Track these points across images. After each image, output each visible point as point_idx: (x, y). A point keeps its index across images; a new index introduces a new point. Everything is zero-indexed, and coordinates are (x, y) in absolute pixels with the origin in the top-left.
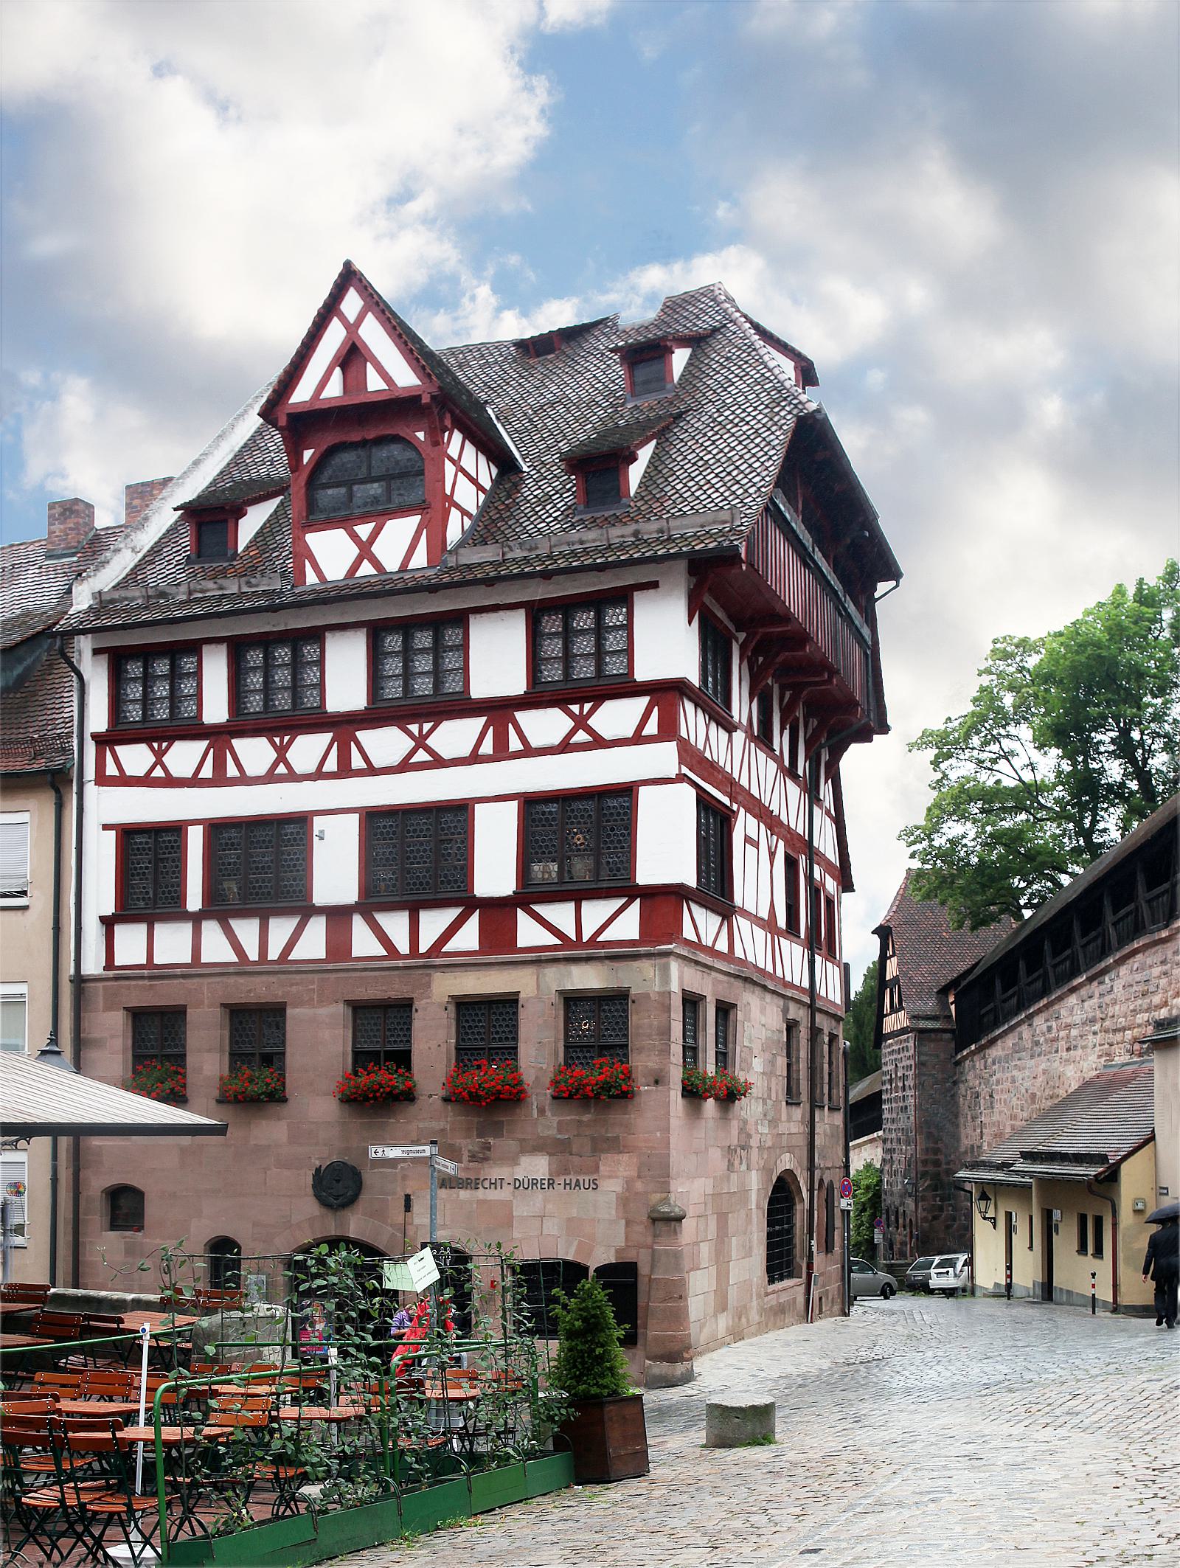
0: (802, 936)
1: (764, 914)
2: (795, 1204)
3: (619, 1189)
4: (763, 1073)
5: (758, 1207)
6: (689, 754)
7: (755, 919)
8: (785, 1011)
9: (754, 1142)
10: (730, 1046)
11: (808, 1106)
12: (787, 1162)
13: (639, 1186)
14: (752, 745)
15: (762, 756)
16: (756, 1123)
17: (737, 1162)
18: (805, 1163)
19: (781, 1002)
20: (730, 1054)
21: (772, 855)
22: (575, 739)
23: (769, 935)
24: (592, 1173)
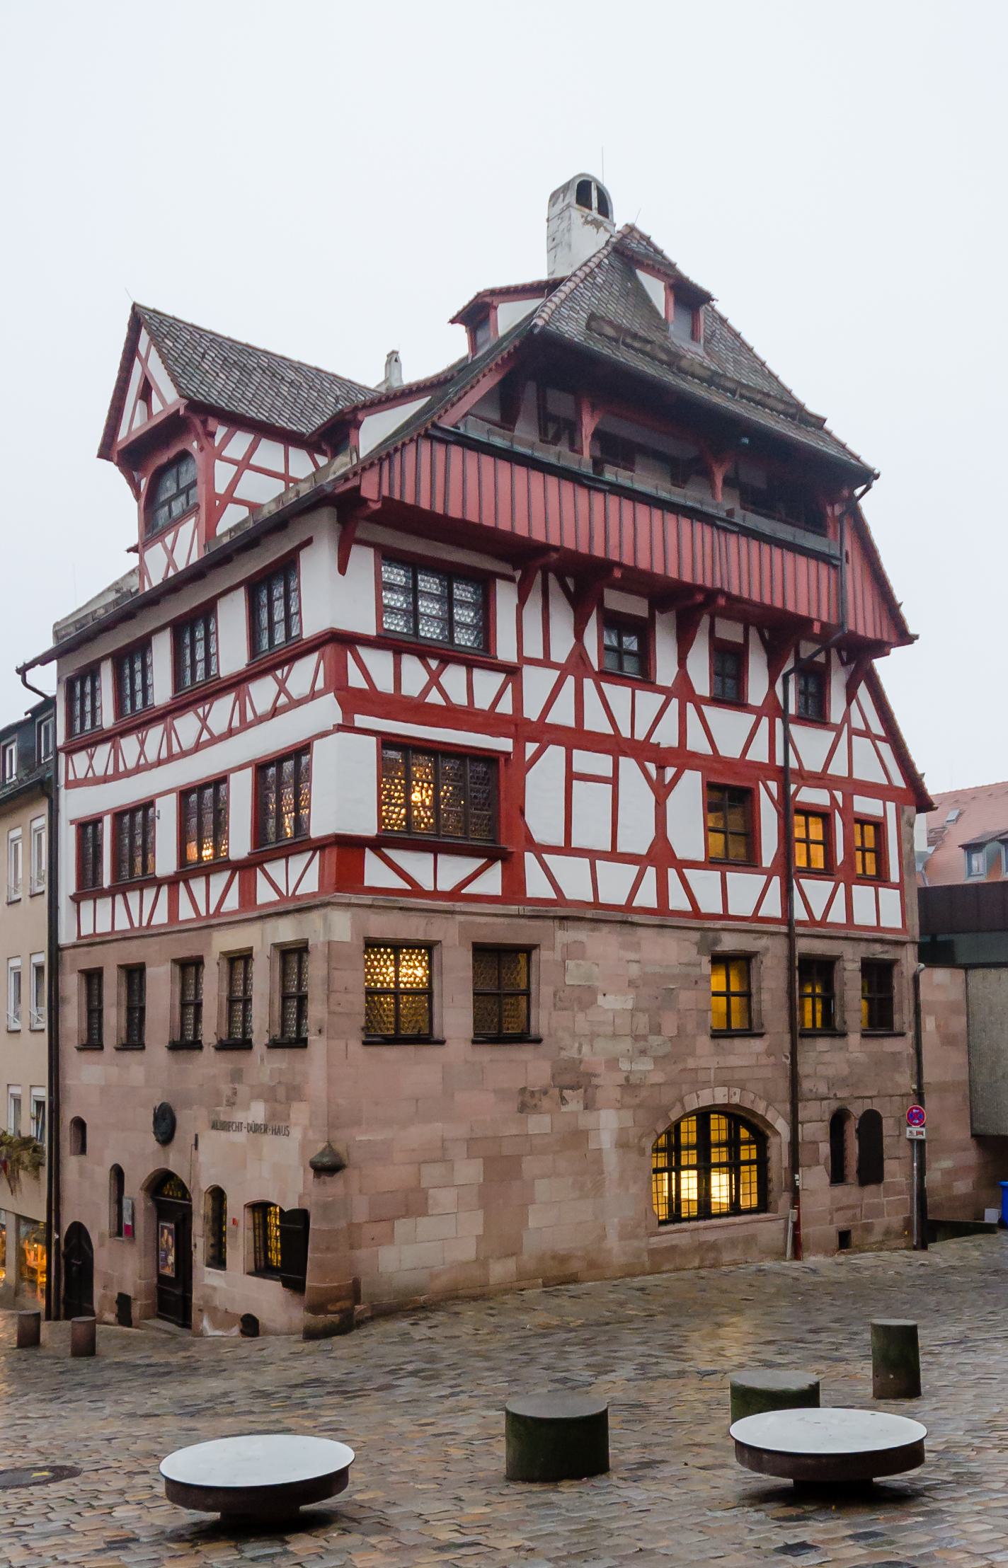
1: (643, 850)
3: (300, 1137)
4: (634, 1011)
6: (368, 701)
7: (614, 855)
9: (608, 1084)
10: (533, 987)
11: (787, 1038)
13: (311, 1135)
14: (589, 684)
16: (613, 1064)
19: (696, 936)
20: (533, 995)
21: (661, 791)
22: (279, 703)
23: (651, 872)
24: (285, 1120)
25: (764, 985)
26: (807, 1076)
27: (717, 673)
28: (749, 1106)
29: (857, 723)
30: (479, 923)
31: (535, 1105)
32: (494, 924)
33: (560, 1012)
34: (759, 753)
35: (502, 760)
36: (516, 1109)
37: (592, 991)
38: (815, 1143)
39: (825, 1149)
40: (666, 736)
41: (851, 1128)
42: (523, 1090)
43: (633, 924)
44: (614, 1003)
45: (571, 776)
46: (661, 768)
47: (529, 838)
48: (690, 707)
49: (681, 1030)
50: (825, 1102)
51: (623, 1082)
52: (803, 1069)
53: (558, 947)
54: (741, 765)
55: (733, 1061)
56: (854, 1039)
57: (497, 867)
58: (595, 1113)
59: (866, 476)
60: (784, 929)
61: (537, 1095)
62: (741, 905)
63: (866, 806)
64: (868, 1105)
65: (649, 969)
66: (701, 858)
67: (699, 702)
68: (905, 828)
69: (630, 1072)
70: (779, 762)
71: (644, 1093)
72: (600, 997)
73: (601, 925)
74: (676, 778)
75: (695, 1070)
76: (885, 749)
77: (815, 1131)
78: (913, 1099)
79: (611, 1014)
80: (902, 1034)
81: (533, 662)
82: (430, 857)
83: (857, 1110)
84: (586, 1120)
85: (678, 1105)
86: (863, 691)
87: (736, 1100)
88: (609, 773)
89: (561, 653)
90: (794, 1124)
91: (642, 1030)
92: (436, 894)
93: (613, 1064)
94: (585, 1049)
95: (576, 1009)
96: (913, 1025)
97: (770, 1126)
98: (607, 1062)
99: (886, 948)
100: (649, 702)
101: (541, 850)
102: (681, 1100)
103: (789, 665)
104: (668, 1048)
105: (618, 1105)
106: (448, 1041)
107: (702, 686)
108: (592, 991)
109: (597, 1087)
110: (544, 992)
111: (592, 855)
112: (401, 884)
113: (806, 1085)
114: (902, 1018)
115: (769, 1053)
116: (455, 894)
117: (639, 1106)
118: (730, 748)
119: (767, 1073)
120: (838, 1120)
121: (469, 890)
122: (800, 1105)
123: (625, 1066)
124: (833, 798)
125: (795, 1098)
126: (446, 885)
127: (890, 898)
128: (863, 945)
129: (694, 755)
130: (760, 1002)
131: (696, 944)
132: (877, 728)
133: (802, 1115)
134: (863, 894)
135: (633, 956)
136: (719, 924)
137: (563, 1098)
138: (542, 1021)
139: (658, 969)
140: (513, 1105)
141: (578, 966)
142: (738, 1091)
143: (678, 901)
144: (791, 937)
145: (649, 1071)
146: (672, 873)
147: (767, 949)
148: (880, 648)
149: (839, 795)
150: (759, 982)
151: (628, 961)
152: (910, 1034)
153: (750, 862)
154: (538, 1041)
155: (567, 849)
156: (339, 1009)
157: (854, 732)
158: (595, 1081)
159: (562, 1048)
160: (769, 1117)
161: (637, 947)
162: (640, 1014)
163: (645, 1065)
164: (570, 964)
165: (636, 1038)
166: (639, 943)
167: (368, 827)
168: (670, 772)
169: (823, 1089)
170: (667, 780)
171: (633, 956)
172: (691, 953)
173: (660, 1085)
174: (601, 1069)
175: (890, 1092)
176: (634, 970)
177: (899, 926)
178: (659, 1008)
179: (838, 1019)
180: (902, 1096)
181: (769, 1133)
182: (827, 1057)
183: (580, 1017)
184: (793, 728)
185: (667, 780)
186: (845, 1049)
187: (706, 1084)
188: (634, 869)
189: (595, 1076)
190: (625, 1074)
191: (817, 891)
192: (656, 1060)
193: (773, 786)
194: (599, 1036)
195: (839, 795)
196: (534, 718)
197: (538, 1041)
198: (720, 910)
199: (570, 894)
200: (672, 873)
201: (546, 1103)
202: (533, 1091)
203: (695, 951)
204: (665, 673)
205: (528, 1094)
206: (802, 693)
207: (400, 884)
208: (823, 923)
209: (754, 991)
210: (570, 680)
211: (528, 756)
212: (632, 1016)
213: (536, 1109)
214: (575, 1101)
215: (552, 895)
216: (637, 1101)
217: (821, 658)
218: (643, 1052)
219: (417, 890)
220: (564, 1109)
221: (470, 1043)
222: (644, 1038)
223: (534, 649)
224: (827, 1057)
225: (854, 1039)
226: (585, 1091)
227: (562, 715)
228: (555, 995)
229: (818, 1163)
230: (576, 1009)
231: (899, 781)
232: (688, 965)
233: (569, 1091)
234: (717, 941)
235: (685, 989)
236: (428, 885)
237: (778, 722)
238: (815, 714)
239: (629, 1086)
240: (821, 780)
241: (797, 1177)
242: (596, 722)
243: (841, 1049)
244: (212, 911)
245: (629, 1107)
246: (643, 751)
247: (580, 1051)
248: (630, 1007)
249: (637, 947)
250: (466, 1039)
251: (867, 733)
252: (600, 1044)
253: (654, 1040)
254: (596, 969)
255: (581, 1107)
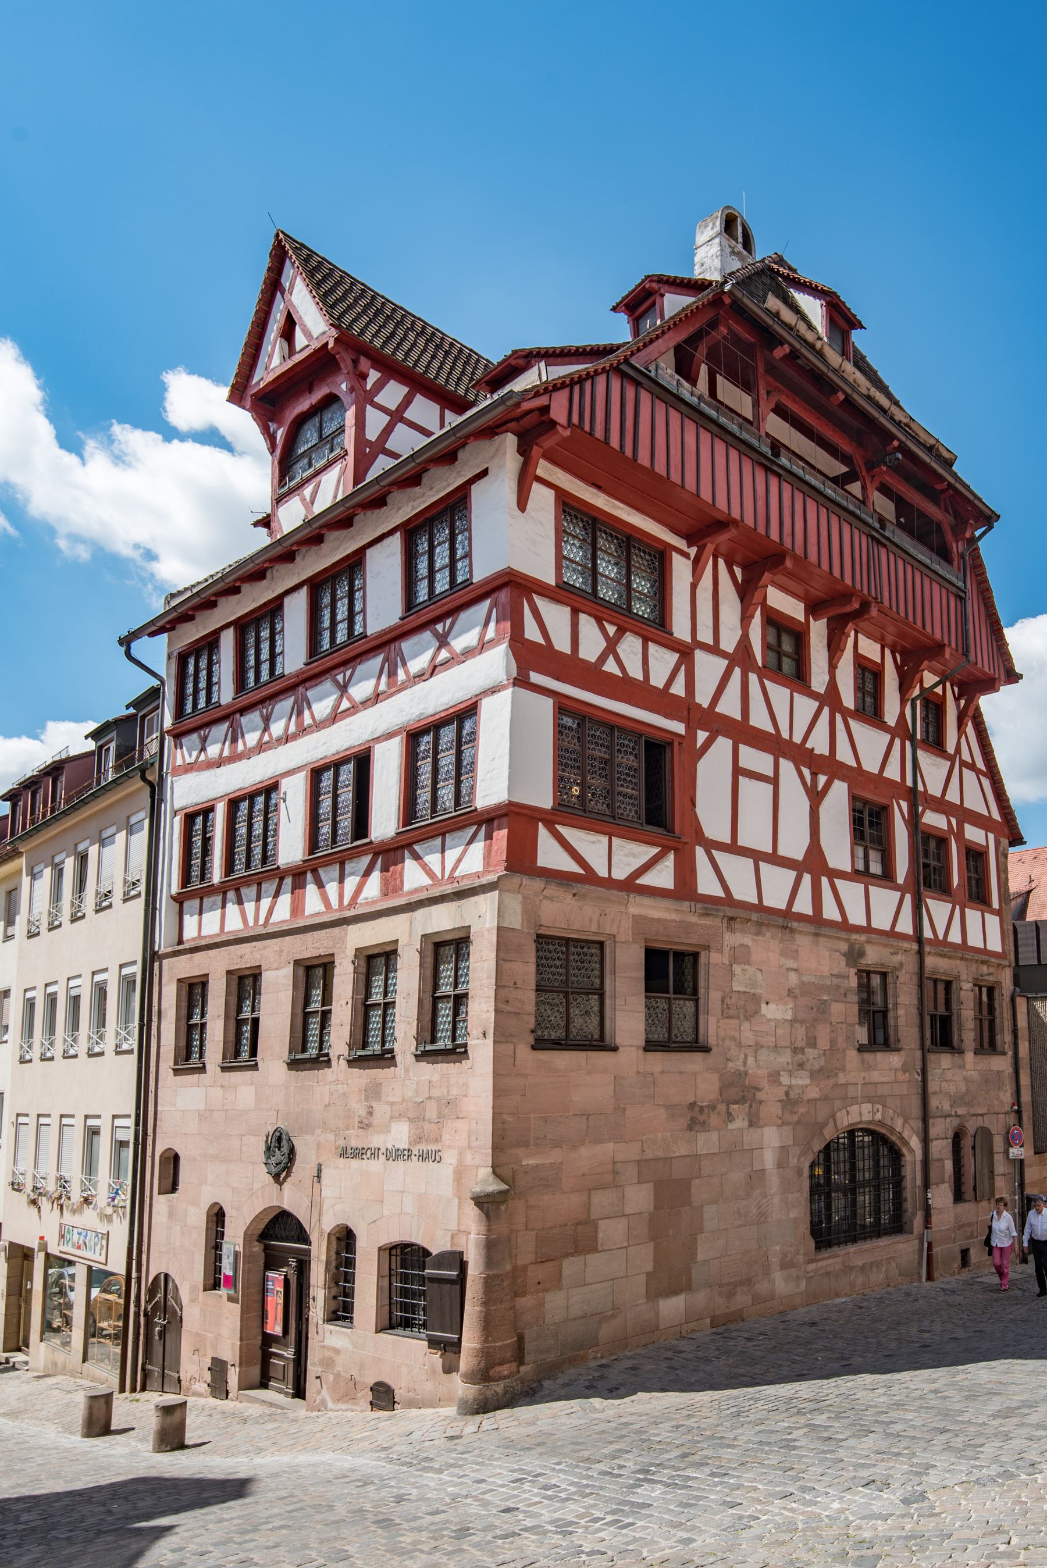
0: (900, 879)
2: (903, 1155)
4: (794, 1021)
5: (781, 1164)
7: (775, 859)
8: (854, 955)
9: (770, 1096)
11: (918, 1054)
12: (862, 1114)
15: (779, 694)
16: (774, 1077)
17: (714, 1120)
18: (916, 1110)
20: (702, 1001)
23: (807, 878)
25: (899, 1000)
26: (935, 1093)
27: (859, 689)
28: (889, 1123)
29: (966, 756)
30: (652, 919)
31: (704, 1122)
32: (666, 920)
33: (727, 1021)
34: (893, 772)
35: (676, 744)
36: (686, 1127)
37: (755, 999)
38: (941, 1160)
39: (949, 1165)
40: (819, 743)
41: (967, 1143)
42: (692, 1105)
43: (792, 931)
44: (775, 1012)
45: (738, 771)
46: (814, 775)
47: (699, 831)
48: (839, 718)
49: (833, 1042)
50: (948, 1120)
51: (784, 1098)
52: (932, 1086)
53: (726, 950)
54: (878, 780)
55: (876, 1076)
56: (969, 1056)
57: (671, 856)
58: (759, 1130)
59: (989, 519)
60: (915, 946)
61: (706, 1110)
62: (882, 921)
63: (974, 834)
64: (980, 1122)
65: (805, 979)
66: (849, 869)
67: (846, 713)
68: (1002, 857)
69: (790, 1087)
70: (909, 783)
71: (802, 1110)
72: (763, 1006)
73: (764, 929)
74: (828, 785)
75: (846, 1085)
76: (986, 783)
77: (941, 1148)
78: (1012, 1119)
79: (773, 1024)
80: (1004, 1054)
81: (704, 647)
82: (605, 839)
83: (971, 1127)
84: (750, 1137)
85: (831, 1120)
86: (970, 729)
87: (879, 1116)
88: (770, 773)
89: (729, 644)
90: (926, 1141)
91: (800, 1043)
92: (609, 883)
93: (774, 1077)
94: (751, 1060)
95: (742, 1018)
96: (1012, 1046)
97: (906, 1143)
98: (770, 1075)
99: (992, 970)
100: (806, 707)
101: (711, 846)
102: (833, 1117)
103: (917, 692)
104: (822, 1062)
105: (780, 1122)
106: (621, 1049)
107: (848, 699)
108: (755, 999)
109: (761, 1102)
110: (712, 996)
111: (757, 856)
112: (574, 868)
113: (934, 1102)
114: (1005, 1038)
115: (905, 1069)
116: (630, 886)
117: (798, 1123)
118: (871, 765)
119: (904, 1089)
120: (957, 1138)
121: (645, 880)
122: (931, 1121)
123: (785, 1079)
124: (949, 823)
125: (925, 1119)
126: (620, 873)
127: (993, 922)
128: (974, 967)
129: (842, 765)
130: (896, 1018)
131: (845, 955)
132: (980, 765)
133: (933, 1132)
134: (973, 916)
135: (792, 964)
136: (863, 938)
137: (729, 1114)
138: (713, 1028)
139: (813, 979)
140: (683, 1122)
141: (744, 970)
142: (880, 1107)
143: (830, 912)
144: (920, 953)
145: (806, 1086)
146: (824, 880)
147: (901, 964)
148: (990, 685)
149: (954, 821)
150: (896, 996)
151: (788, 969)
152: (1010, 1053)
153: (887, 877)
154: (706, 1049)
155: (733, 848)
156: (509, 1008)
157: (963, 764)
158: (760, 1096)
159: (728, 1060)
160: (905, 1135)
161: (795, 955)
162: (797, 1025)
163: (802, 1080)
164: (737, 969)
165: (795, 1051)
166: (797, 951)
167: (544, 799)
168: (822, 779)
169: (946, 1106)
170: (820, 788)
171: (792, 964)
172: (840, 965)
173: (815, 1100)
174: (765, 1084)
175: (997, 1110)
176: (793, 979)
177: (1000, 950)
178: (815, 1020)
179: (956, 1038)
180: (1006, 1113)
181: (904, 1151)
182: (949, 1075)
183: (746, 1025)
184: (921, 754)
185: (820, 788)
186: (962, 1067)
187: (854, 1101)
188: (793, 874)
189: (760, 1090)
190: (786, 1089)
191: (939, 910)
192: (813, 1075)
193: (904, 805)
194: (762, 1047)
195: (954, 821)
196: (705, 705)
197: (706, 1049)
198: (864, 923)
199: (738, 895)
200: (824, 880)
201: (714, 1120)
202: (702, 1107)
203: (843, 963)
204: (819, 681)
205: (697, 1109)
206: (925, 719)
207: (574, 868)
208: (945, 943)
209: (890, 1006)
210: (737, 672)
211: (699, 744)
212: (792, 1026)
213: (704, 1126)
214: (741, 1117)
215: (721, 894)
216: (796, 1118)
217: (939, 690)
218: (801, 1066)
219: (590, 877)
220: (731, 1126)
221: (641, 1052)
222: (802, 1050)
223: (705, 636)
224: (949, 1075)
225: (969, 1056)
226: (751, 1106)
227: (729, 706)
228: (723, 1001)
229: (943, 1182)
230: (742, 1018)
231: (996, 816)
232: (838, 976)
233: (736, 1107)
234: (862, 954)
235: (837, 1001)
236: (603, 872)
237: (908, 744)
238: (936, 744)
239: (789, 1102)
240: (940, 805)
241: (929, 1195)
242: (759, 720)
243: (960, 1067)
244: (346, 902)
245: (788, 1124)
246: (801, 755)
247: (745, 1063)
248: (789, 1018)
249: (795, 955)
250: (638, 1047)
251: (972, 767)
252: (764, 1055)
253: (811, 1053)
254: (759, 974)
255: (746, 1123)
